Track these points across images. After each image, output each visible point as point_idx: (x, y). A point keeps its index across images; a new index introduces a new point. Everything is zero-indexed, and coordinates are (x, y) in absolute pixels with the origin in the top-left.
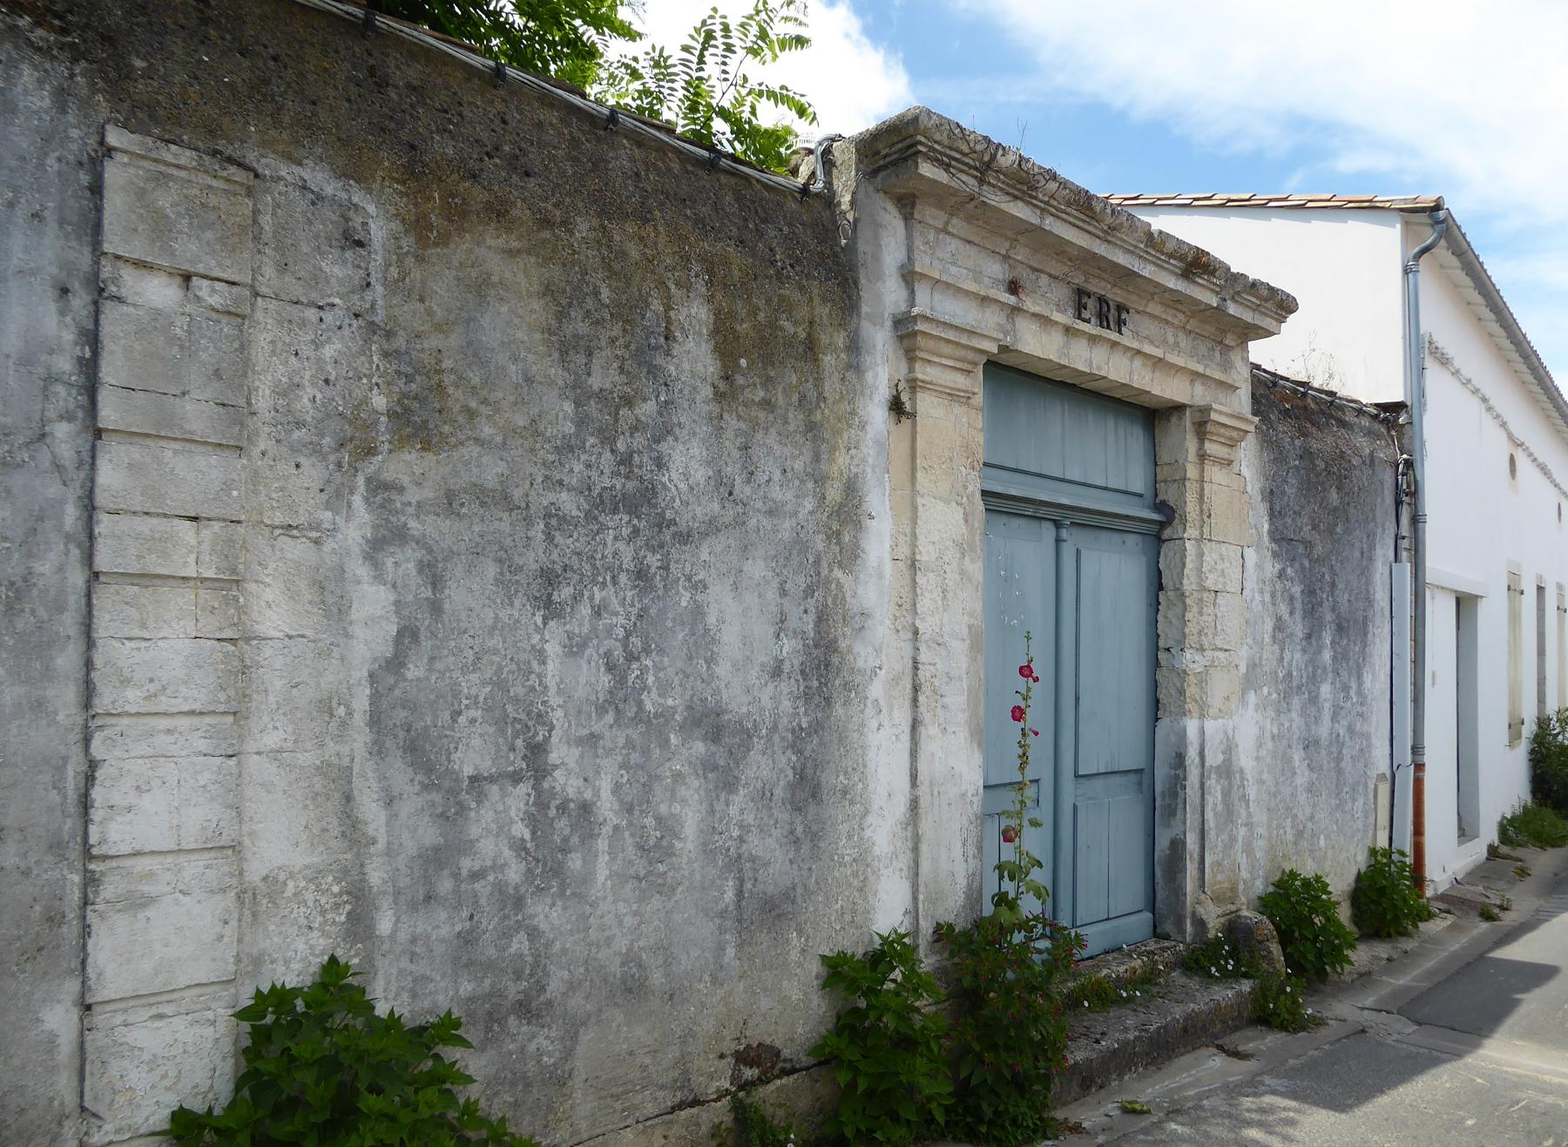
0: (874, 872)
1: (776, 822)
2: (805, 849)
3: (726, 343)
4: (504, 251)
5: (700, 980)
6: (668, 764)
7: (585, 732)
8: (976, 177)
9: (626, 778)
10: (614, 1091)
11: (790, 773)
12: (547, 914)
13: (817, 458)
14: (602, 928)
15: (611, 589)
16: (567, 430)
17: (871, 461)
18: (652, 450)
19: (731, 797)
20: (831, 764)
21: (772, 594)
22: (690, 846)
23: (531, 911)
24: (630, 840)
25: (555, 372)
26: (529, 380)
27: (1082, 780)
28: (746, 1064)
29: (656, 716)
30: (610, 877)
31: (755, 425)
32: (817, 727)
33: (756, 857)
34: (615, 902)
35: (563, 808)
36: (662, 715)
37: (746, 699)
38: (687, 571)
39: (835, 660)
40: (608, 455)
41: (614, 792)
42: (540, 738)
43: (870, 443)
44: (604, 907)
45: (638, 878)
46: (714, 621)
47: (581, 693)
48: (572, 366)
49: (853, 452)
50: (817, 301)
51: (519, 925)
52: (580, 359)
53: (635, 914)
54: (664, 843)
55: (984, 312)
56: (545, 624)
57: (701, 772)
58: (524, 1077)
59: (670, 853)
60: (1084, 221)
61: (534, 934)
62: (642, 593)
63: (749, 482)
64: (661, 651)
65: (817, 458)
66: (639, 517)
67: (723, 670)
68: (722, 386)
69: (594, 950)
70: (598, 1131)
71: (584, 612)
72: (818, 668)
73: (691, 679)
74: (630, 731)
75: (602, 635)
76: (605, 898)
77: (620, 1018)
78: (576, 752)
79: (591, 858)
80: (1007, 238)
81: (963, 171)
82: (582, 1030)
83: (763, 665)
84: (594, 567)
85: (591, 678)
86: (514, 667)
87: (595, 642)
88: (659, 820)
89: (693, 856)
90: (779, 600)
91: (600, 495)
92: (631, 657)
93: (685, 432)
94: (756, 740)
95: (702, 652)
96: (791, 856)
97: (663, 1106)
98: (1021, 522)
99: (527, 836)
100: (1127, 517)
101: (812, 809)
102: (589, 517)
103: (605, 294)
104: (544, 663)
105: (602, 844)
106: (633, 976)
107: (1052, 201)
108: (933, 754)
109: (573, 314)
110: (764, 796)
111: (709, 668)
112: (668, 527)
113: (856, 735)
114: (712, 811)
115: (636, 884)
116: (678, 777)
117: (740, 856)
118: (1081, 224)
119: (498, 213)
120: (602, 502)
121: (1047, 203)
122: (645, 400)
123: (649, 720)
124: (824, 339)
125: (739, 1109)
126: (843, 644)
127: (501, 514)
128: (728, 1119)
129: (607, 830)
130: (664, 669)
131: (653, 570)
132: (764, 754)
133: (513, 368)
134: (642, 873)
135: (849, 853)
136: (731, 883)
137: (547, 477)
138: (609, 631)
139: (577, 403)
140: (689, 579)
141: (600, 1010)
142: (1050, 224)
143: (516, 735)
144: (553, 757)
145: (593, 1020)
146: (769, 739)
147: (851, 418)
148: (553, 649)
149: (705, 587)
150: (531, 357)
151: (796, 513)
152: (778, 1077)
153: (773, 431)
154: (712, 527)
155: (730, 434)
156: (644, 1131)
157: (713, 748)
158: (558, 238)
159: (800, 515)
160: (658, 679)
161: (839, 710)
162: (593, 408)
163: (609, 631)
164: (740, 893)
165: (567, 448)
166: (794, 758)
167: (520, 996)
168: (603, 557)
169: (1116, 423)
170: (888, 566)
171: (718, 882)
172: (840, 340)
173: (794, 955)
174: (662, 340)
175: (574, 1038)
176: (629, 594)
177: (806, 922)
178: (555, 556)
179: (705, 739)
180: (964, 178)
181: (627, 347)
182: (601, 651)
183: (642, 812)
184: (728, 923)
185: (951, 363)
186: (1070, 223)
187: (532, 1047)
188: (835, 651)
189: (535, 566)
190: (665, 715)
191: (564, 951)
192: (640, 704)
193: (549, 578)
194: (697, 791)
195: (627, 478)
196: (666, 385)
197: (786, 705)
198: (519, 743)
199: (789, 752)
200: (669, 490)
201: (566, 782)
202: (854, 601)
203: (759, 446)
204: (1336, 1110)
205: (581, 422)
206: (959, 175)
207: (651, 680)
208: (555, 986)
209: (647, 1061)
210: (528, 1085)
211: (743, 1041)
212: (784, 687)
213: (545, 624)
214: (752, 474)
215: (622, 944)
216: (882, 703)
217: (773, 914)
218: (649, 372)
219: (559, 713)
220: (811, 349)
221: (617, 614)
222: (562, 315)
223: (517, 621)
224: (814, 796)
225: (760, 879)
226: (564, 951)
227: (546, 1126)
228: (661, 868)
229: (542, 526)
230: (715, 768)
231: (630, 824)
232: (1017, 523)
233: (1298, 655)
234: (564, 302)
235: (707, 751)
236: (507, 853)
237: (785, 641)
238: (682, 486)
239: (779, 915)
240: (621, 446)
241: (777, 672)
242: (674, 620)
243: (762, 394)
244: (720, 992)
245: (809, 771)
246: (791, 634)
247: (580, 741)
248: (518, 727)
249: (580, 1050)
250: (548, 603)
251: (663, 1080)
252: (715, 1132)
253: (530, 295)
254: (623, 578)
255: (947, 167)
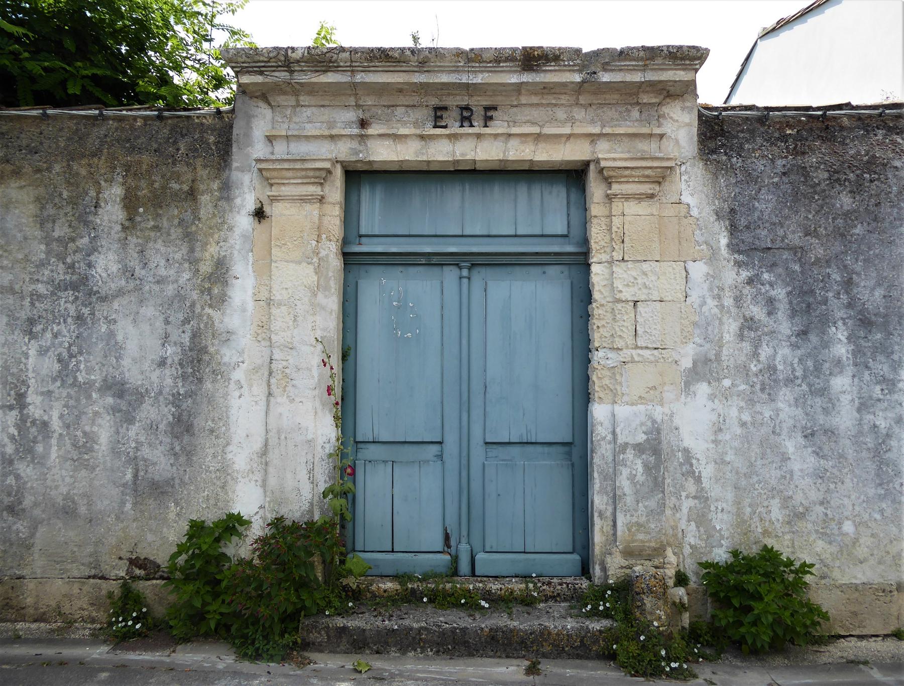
0: (233, 479)
1: (161, 442)
2: (182, 459)
3: (130, 203)
4: (18, 188)
5: (109, 516)
6: (90, 407)
7: (46, 389)
8: (286, 71)
9: (66, 412)
10: (56, 559)
11: (171, 418)
12: (25, 469)
13: (192, 250)
14: (54, 481)
15: (63, 325)
16: (41, 257)
17: (237, 247)
18: (85, 259)
19: (130, 427)
20: (202, 415)
21: (159, 324)
22: (103, 448)
23: (17, 467)
24: (68, 441)
25: (38, 233)
26: (26, 238)
27: (490, 446)
28: (136, 566)
29: (84, 384)
30: (58, 457)
31: (148, 239)
32: (191, 394)
33: (147, 459)
34: (61, 469)
35: (34, 422)
36: (87, 383)
37: (140, 377)
38: (105, 314)
39: (206, 358)
40: (61, 265)
41: (60, 418)
42: (23, 391)
43: (237, 237)
44: (54, 471)
45: (73, 459)
46: (122, 338)
47: (44, 372)
48: (45, 229)
49: (222, 244)
50: (199, 168)
51: (10, 473)
52: (50, 225)
53: (71, 477)
54: (88, 445)
55: (396, 145)
56: (29, 342)
57: (111, 412)
58: (10, 540)
59: (91, 450)
60: (395, 66)
61: (18, 477)
62: (79, 326)
63: (144, 268)
64: (89, 353)
65: (192, 250)
66: (78, 292)
67: (126, 362)
68: (127, 224)
69: (48, 490)
70: (47, 576)
71: (48, 336)
72: (192, 362)
73: (106, 366)
74: (69, 390)
75: (57, 346)
76: (55, 467)
77: (60, 525)
78: (40, 398)
79: (48, 447)
80: (350, 95)
81: (274, 71)
82: (40, 525)
83: (153, 360)
84: (54, 316)
85: (50, 365)
86: (13, 360)
87: (53, 349)
88: (85, 433)
89: (105, 453)
90: (164, 327)
91: (59, 284)
92: (71, 356)
93: (105, 249)
94: (146, 398)
95: (113, 354)
96: (172, 461)
97: (83, 574)
98: (421, 269)
99: (16, 434)
100: (537, 254)
101: (186, 438)
102: (53, 294)
103: (65, 194)
104: (28, 359)
105: (54, 441)
106: (69, 506)
107: (354, 64)
108: (281, 414)
109: (47, 207)
110: (152, 428)
111: (117, 361)
112: (95, 294)
113: (222, 400)
114: (118, 433)
115: (72, 462)
116: (96, 414)
117: (136, 458)
118: (392, 69)
119: (17, 173)
120: (60, 287)
121: (350, 66)
122: (82, 237)
123: (80, 385)
124: (202, 187)
125: (125, 587)
126: (212, 349)
127: (9, 296)
128: (117, 592)
129: (56, 435)
130: (90, 361)
131: (86, 315)
132: (153, 406)
133: (19, 235)
134: (75, 458)
135: (214, 465)
136: (130, 470)
137: (31, 278)
138: (61, 344)
139: (47, 245)
140: (106, 318)
141: (50, 519)
142: (359, 78)
143: (11, 389)
144: (29, 400)
145: (45, 522)
146: (156, 398)
147: (222, 225)
148: (32, 352)
149: (115, 322)
150: (27, 229)
151: (177, 281)
152: (157, 579)
153: (160, 241)
154: (120, 293)
155: (132, 246)
156: (68, 583)
157: (118, 401)
158: (45, 176)
159: (180, 282)
160: (86, 366)
161: (208, 385)
162: (54, 245)
163: (61, 344)
164: (136, 476)
165: (42, 264)
166: (173, 409)
167: (10, 504)
168: (59, 311)
169: (529, 189)
170: (250, 305)
171: (122, 469)
172: (215, 185)
173: (172, 516)
174: (93, 208)
175: (36, 528)
176: (72, 327)
177: (181, 499)
178: (35, 312)
179: (114, 396)
180: (276, 74)
181: (73, 215)
182: (56, 353)
183: (75, 428)
184: (128, 491)
185: (300, 181)
186: (382, 71)
187: (15, 528)
188: (206, 352)
189: (26, 317)
190: (90, 384)
191: (32, 488)
192: (75, 378)
193: (31, 322)
194: (108, 421)
195: (72, 274)
196: (94, 229)
197: (169, 381)
198: (12, 393)
199: (170, 406)
200: (95, 277)
201: (35, 410)
202: (221, 325)
203: (151, 249)
204: (284, 659)
205: (48, 253)
206: (273, 74)
207: (82, 366)
208: (28, 501)
209: (75, 549)
210: (11, 544)
211: (134, 554)
212: (168, 372)
213: (29, 342)
214: (146, 264)
215: (64, 490)
216: (243, 382)
217: (158, 491)
218: (84, 225)
219: (33, 380)
220: (192, 194)
221: (65, 336)
222: (43, 208)
223: (16, 341)
224: (187, 431)
225: (149, 471)
226: (32, 488)
227: (19, 566)
228: (86, 457)
229: (29, 300)
230: (120, 411)
231: (68, 434)
232: (412, 270)
233: (785, 351)
234: (44, 202)
235: (114, 402)
236: (6, 440)
237: (168, 347)
238: (104, 275)
239: (161, 492)
240: (69, 260)
241: (162, 363)
242: (97, 338)
243: (152, 223)
244: (121, 525)
245: (185, 418)
246: (172, 344)
247: (42, 393)
248: (12, 386)
249: (38, 535)
250: (31, 332)
251: (84, 561)
252: (110, 595)
253: (29, 203)
254: (69, 320)
255: (261, 73)
